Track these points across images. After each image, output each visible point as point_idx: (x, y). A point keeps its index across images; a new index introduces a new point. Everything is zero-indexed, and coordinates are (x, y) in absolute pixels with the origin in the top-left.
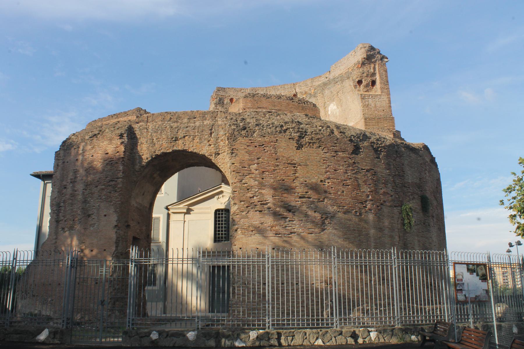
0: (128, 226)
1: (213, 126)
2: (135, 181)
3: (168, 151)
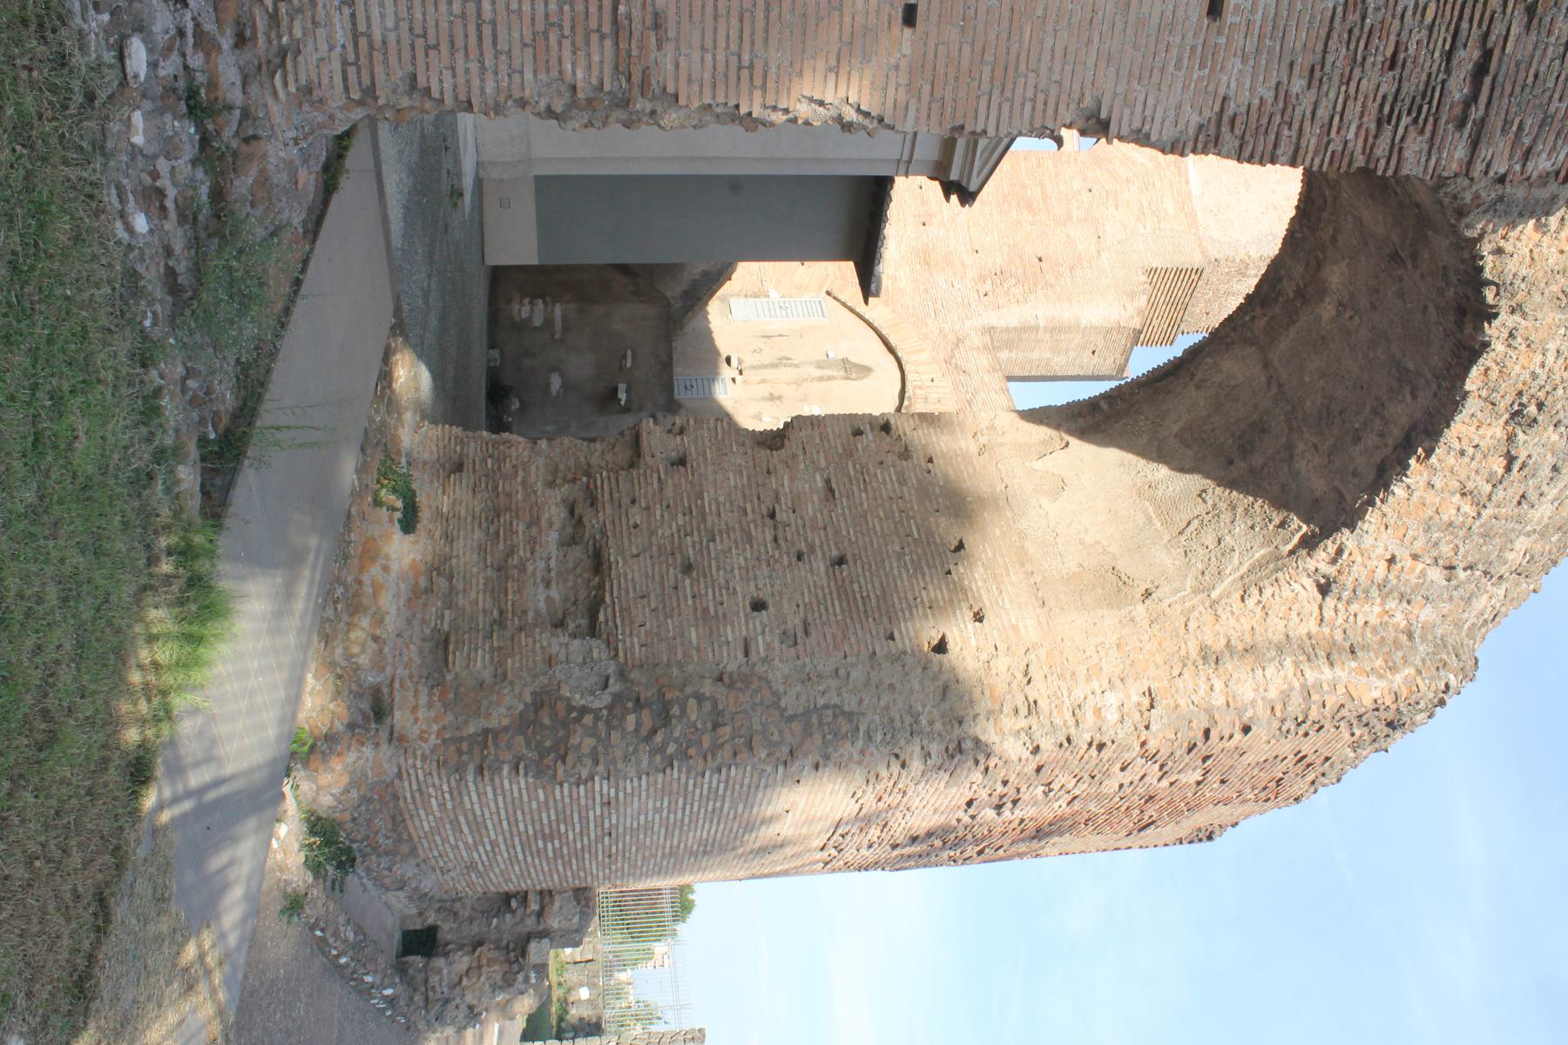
1: (1485, 573)
3: (1475, 372)
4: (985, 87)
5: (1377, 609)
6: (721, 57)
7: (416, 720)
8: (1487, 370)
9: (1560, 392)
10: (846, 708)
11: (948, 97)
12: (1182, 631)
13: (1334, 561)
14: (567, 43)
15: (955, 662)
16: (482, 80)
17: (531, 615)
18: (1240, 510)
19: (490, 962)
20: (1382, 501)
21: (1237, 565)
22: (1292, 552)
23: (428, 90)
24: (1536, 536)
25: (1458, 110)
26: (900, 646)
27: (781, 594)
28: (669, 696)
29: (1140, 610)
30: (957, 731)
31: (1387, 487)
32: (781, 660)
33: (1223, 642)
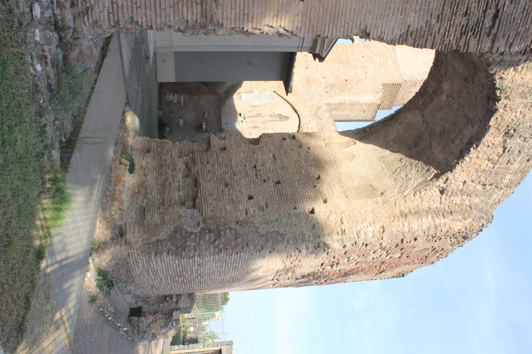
1: (496, 187)
3: (493, 119)
4: (328, 22)
5: (460, 199)
6: (238, 11)
7: (134, 237)
8: (497, 118)
9: (521, 126)
10: (280, 232)
11: (315, 25)
12: (394, 206)
13: (445, 183)
14: (185, 6)
15: (317, 216)
16: (156, 19)
17: (173, 201)
18: (413, 165)
19: (160, 319)
20: (462, 162)
21: (413, 184)
22: (431, 180)
23: (137, 22)
24: (513, 174)
25: (488, 30)
26: (299, 211)
27: (258, 193)
28: (220, 228)
29: (380, 199)
30: (318, 240)
31: (463, 158)
32: (258, 216)
33: (408, 210)
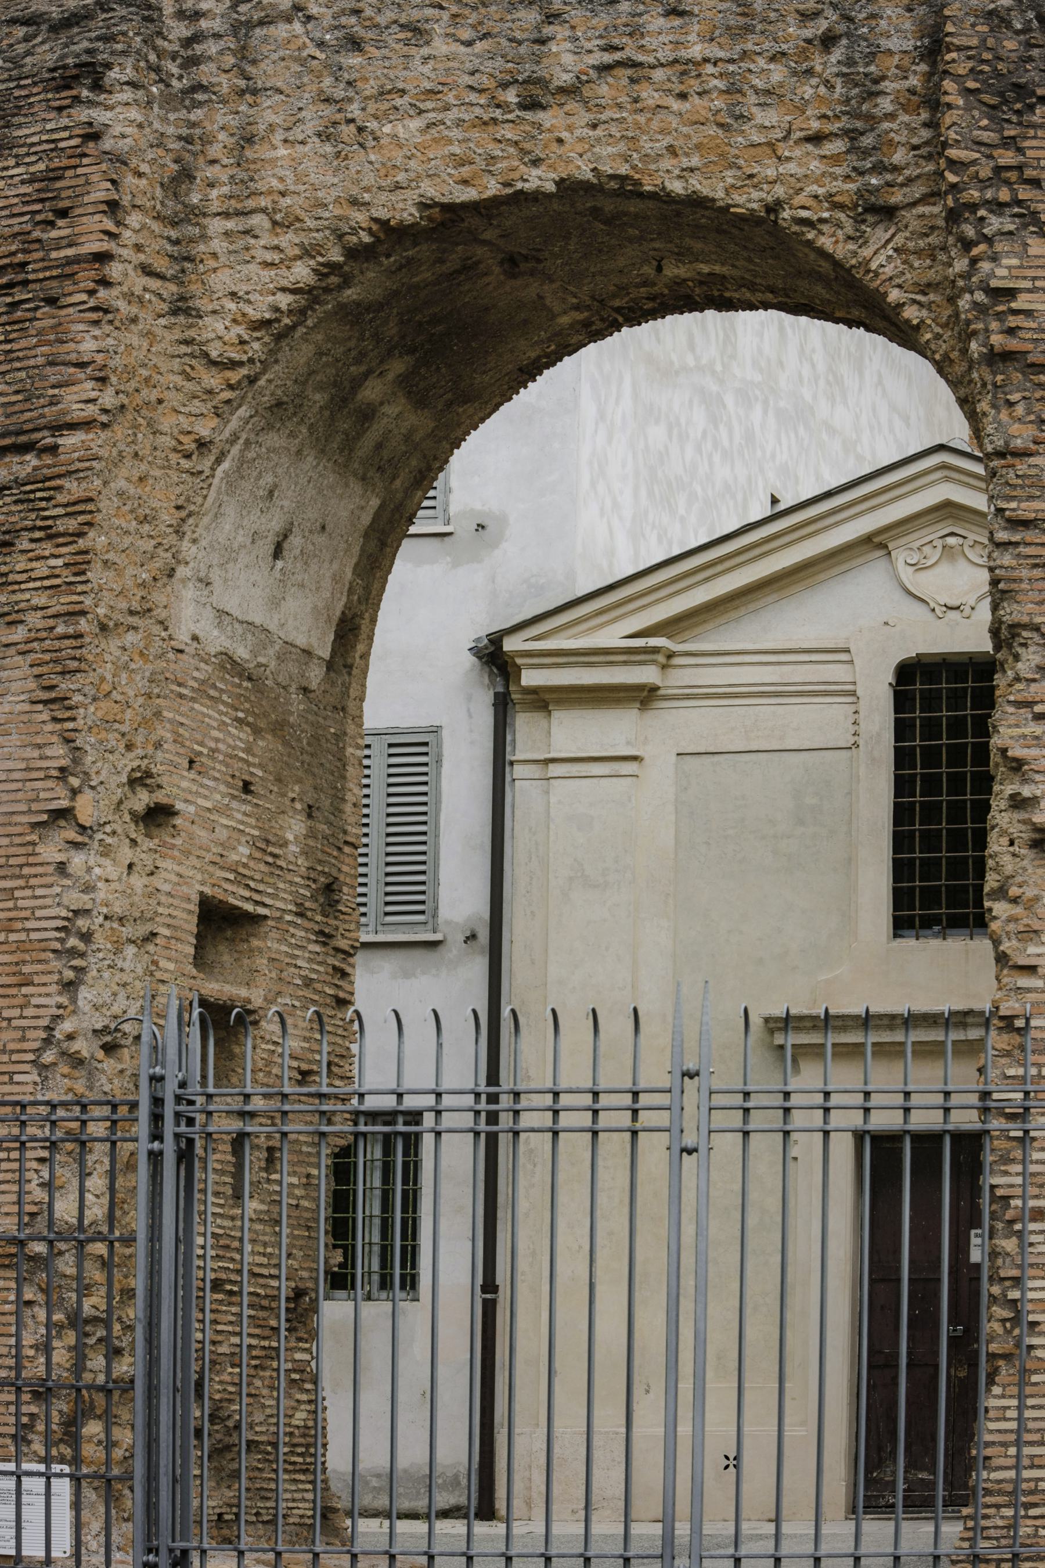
0: (158, 816)
2: (202, 445)
3: (470, 194)
